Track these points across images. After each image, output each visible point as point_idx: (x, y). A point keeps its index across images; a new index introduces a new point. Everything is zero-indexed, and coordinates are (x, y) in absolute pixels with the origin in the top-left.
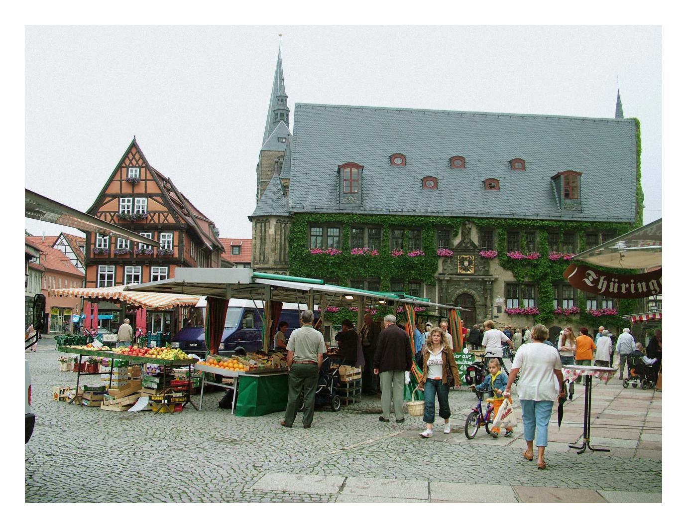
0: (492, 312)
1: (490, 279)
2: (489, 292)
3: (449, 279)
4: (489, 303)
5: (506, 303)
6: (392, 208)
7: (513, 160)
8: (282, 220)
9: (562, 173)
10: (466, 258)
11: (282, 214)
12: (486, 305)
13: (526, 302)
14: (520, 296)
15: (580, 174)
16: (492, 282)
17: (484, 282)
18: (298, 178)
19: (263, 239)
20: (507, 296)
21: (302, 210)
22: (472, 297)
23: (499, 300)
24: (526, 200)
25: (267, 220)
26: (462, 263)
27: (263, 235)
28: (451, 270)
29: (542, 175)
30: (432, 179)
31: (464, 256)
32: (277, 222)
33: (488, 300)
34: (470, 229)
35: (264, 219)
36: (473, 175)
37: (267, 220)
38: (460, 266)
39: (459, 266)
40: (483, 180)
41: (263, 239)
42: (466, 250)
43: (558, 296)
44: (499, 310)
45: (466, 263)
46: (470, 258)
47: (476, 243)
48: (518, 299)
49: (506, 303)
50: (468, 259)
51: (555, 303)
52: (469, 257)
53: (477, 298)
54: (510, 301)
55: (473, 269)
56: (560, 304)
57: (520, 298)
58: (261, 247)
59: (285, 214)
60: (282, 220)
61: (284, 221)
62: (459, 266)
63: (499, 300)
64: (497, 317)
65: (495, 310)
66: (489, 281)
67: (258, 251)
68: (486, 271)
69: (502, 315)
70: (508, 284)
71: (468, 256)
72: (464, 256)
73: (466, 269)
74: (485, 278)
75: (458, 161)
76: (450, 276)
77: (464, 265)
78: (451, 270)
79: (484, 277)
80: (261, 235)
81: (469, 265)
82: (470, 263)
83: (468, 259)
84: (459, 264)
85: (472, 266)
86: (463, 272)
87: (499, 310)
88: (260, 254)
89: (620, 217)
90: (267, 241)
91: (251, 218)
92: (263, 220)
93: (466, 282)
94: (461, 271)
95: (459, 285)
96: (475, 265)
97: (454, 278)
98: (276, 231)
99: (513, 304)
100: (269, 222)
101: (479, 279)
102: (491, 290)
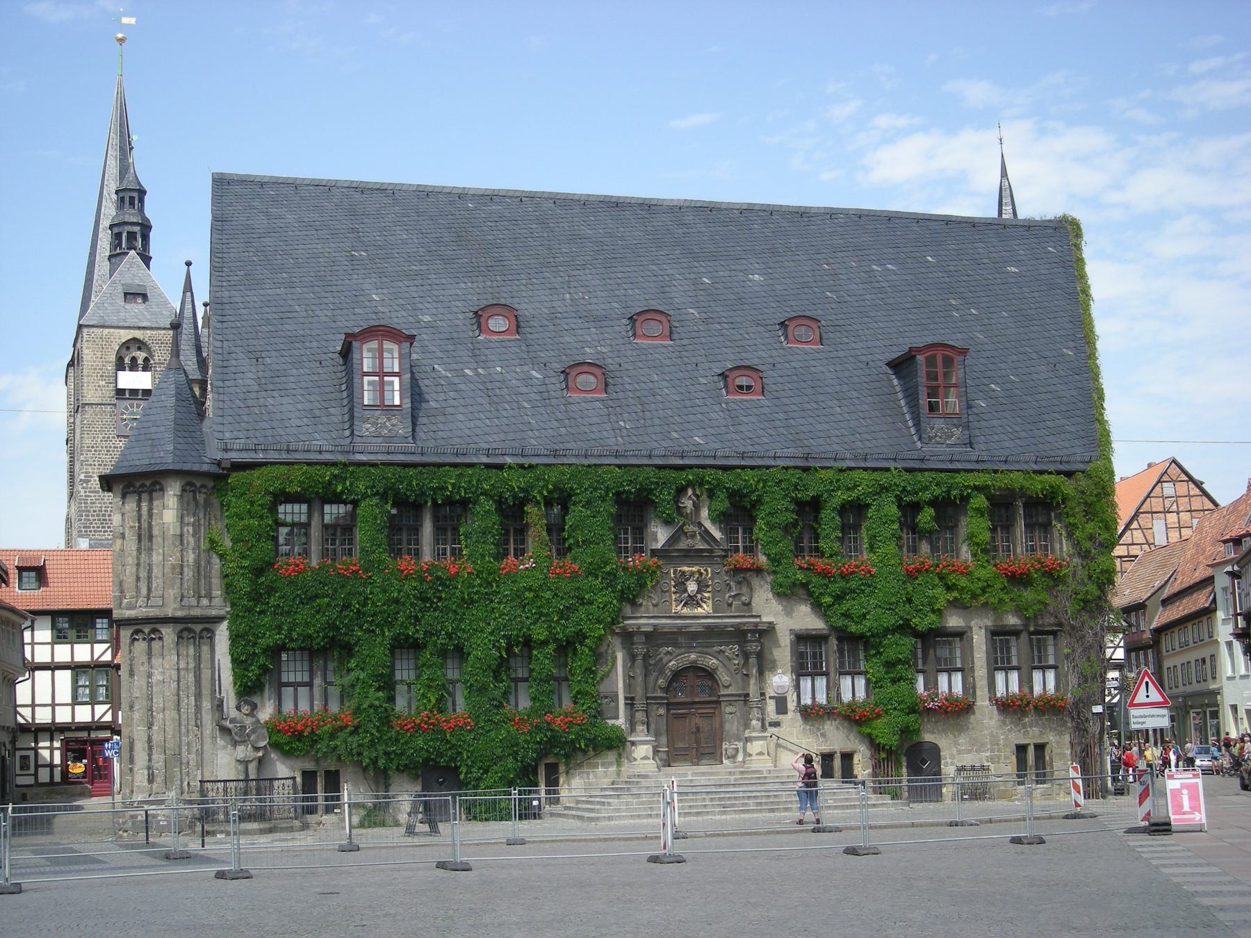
0: (762, 710)
1: (756, 624)
2: (753, 660)
3: (650, 629)
4: (753, 689)
5: (797, 687)
6: (494, 445)
7: (790, 319)
8: (198, 485)
9: (920, 350)
10: (692, 574)
11: (196, 468)
12: (747, 695)
13: (846, 682)
14: (832, 669)
15: (964, 352)
16: (762, 633)
17: (739, 635)
18: (233, 369)
19: (145, 536)
20: (801, 670)
21: (253, 455)
22: (709, 674)
23: (780, 680)
24: (837, 421)
25: (154, 484)
26: (681, 586)
27: (145, 525)
29: (864, 358)
30: (592, 369)
31: (686, 569)
32: (184, 490)
33: (752, 681)
35: (148, 483)
36: (694, 360)
37: (154, 484)
39: (674, 597)
40: (720, 372)
41: (145, 536)
42: (691, 555)
43: (963, 662)
44: (782, 707)
45: (692, 587)
46: (701, 574)
47: (718, 535)
48: (826, 674)
49: (797, 687)
51: (921, 680)
52: (699, 572)
53: (724, 677)
54: (806, 683)
55: (710, 602)
56: (931, 684)
57: (832, 675)
58: (138, 559)
59: (205, 468)
60: (198, 485)
61: (203, 486)
62: (674, 597)
63: (780, 680)
64: (776, 724)
65: (771, 706)
66: (753, 632)
67: (130, 570)
68: (744, 604)
69: (792, 717)
70: (801, 638)
71: (694, 569)
72: (686, 569)
73: (692, 601)
74: (745, 624)
75: (652, 322)
76: (652, 621)
77: (686, 590)
79: (738, 620)
80: (140, 528)
81: (699, 591)
82: (702, 586)
86: (686, 611)
87: (782, 707)
88: (138, 579)
89: (1065, 459)
90: (157, 541)
91: (107, 482)
92: (143, 485)
93: (694, 636)
95: (676, 645)
96: (714, 592)
97: (664, 625)
98: (181, 519)
99: (815, 691)
100: (162, 490)
101: (726, 626)
102: (760, 656)
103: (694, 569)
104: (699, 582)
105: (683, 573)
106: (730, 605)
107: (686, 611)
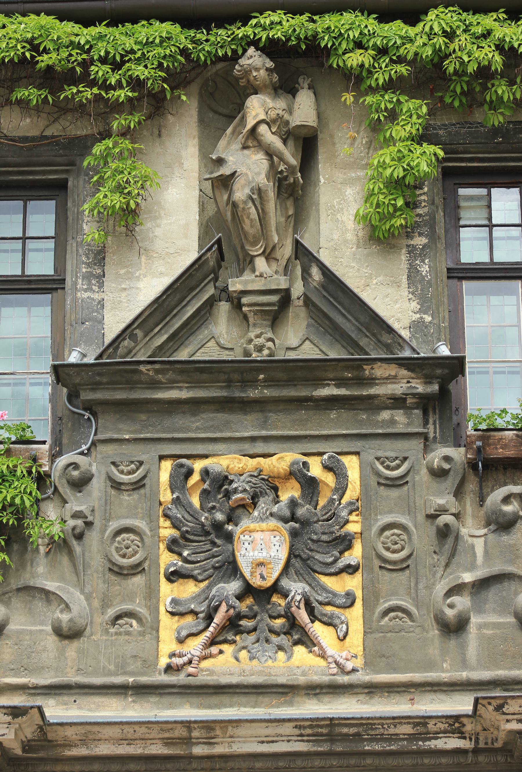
26: (208, 540)
28: (69, 634)
31: (228, 462)
34: (307, 144)
38: (189, 590)
39: (167, 591)
45: (261, 546)
46: (310, 486)
50: (290, 492)
55: (355, 616)
71: (282, 460)
78: (69, 634)
82: (315, 542)
83: (290, 492)
84: (167, 560)
85: (335, 584)
86: (228, 663)
94: (194, 646)
97: (90, 729)
103: (282, 460)
104: (298, 526)
105: (218, 484)
106: (454, 628)
107: (228, 663)
